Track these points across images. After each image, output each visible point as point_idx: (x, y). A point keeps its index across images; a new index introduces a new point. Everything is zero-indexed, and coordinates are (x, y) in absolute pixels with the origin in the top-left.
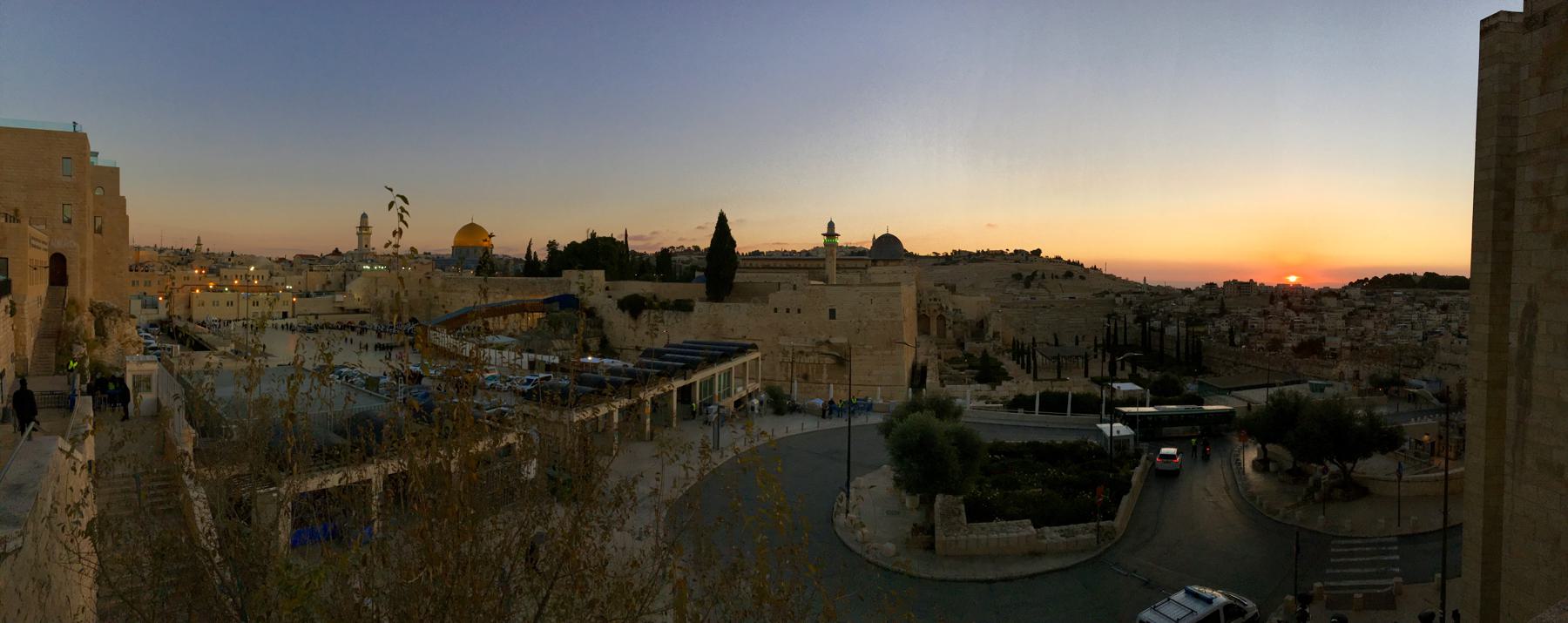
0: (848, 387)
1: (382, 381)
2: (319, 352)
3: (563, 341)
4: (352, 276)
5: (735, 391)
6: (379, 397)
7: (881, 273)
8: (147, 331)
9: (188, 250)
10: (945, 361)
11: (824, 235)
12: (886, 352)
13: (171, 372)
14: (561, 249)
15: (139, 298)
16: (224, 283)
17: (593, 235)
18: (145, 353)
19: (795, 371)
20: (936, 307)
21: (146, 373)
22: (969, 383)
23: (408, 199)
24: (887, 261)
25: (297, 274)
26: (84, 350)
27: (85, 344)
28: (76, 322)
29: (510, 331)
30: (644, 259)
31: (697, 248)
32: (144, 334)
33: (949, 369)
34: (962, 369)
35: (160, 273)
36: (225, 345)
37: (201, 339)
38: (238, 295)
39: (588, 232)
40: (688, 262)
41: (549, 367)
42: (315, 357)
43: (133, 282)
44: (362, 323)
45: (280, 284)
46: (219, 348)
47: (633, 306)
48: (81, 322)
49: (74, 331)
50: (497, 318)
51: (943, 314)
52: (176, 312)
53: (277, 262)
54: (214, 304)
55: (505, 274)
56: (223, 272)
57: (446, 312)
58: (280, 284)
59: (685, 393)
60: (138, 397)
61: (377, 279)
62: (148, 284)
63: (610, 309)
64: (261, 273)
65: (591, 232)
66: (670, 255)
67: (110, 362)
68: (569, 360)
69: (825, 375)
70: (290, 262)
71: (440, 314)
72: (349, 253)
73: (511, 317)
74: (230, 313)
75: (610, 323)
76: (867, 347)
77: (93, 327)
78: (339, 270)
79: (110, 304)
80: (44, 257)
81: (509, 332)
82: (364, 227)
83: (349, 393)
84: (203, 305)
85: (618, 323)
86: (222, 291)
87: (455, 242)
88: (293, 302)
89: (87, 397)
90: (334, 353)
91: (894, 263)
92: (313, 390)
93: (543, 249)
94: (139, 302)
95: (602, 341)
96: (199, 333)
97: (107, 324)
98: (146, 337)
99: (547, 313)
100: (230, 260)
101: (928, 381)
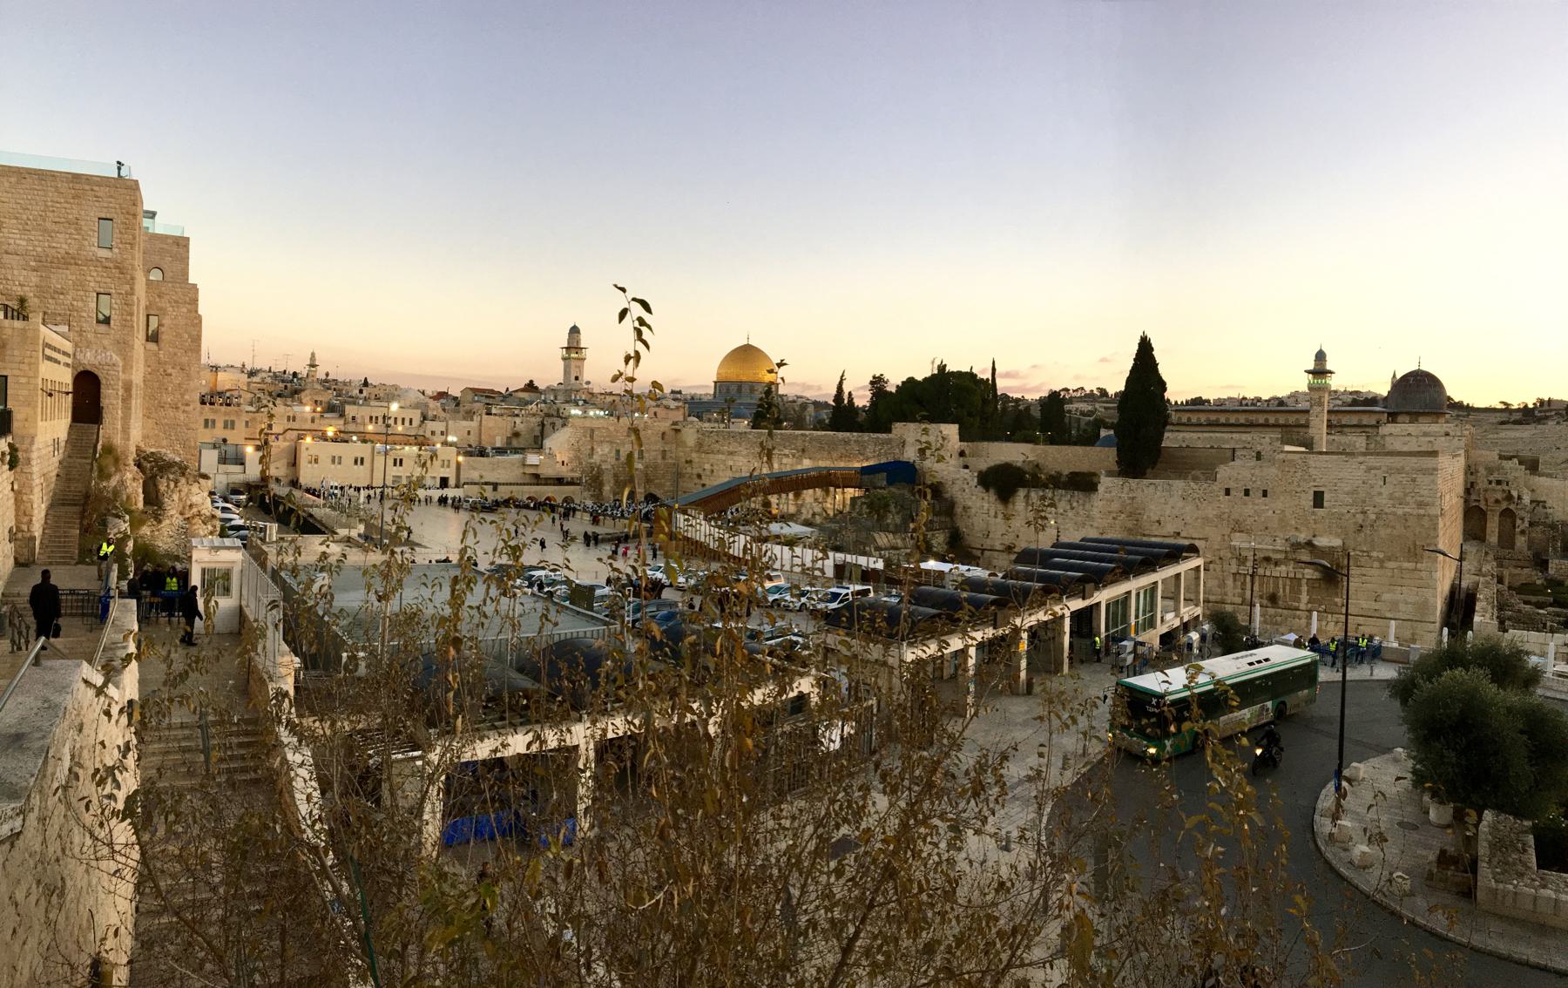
0: (1343, 618)
2: (501, 544)
3: (891, 536)
5: (1162, 618)
7: (1400, 434)
8: (226, 500)
9: (295, 374)
10: (1510, 588)
11: (1308, 372)
12: (1406, 565)
13: (263, 565)
15: (215, 447)
17: (942, 368)
18: (222, 535)
19: (1256, 588)
20: (1499, 496)
22: (1552, 631)
23: (651, 306)
24: (1414, 416)
26: (125, 526)
27: (127, 517)
28: (114, 481)
29: (806, 514)
30: (1021, 407)
31: (1103, 392)
32: (221, 504)
33: (1516, 600)
34: (1540, 605)
35: (250, 408)
37: (311, 516)
38: (373, 448)
40: (1090, 413)
41: (867, 576)
42: (495, 551)
43: (206, 421)
45: (438, 432)
47: (1002, 482)
48: (122, 482)
49: (110, 495)
50: (784, 496)
51: (1512, 507)
54: (333, 462)
55: (799, 424)
57: (704, 485)
59: (1083, 620)
60: (213, 603)
61: (592, 431)
62: (230, 425)
63: (966, 486)
66: (1063, 401)
67: (166, 547)
68: (899, 566)
69: (1304, 597)
71: (694, 490)
73: (808, 495)
75: (966, 508)
76: (1374, 554)
77: (140, 490)
79: (170, 455)
81: (803, 517)
85: (979, 509)
87: (718, 374)
89: (127, 600)
90: (524, 545)
91: (1429, 419)
92: (488, 601)
94: (215, 453)
95: (951, 533)
96: (308, 506)
97: (162, 488)
98: (224, 510)
99: (867, 490)
101: (1477, 619)
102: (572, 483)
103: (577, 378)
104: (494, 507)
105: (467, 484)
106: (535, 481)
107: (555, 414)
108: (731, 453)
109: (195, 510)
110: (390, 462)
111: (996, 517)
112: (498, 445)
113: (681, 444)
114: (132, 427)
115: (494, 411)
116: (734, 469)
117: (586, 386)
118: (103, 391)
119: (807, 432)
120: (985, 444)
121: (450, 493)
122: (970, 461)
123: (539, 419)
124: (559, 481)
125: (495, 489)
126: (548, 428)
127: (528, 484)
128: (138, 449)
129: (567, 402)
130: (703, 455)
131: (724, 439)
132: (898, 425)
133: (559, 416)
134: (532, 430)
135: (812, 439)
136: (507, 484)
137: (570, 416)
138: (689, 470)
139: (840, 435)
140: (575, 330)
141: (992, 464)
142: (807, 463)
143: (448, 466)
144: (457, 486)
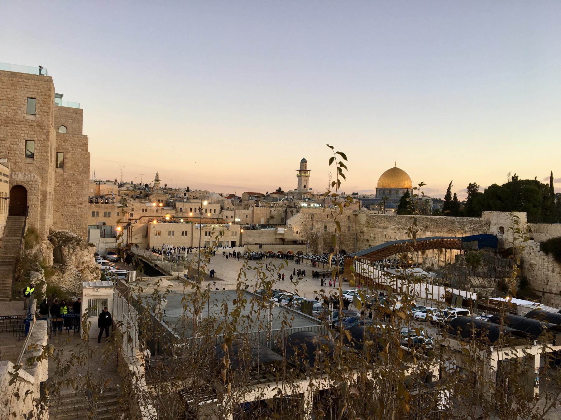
1: (315, 305)
2: (260, 281)
3: (481, 280)
4: (292, 212)
6: (312, 320)
8: (105, 258)
14: (481, 191)
15: (98, 228)
16: (180, 215)
21: (102, 297)
25: (244, 209)
26: (41, 276)
27: (43, 271)
28: (35, 250)
32: (102, 261)
36: (179, 271)
37: (156, 265)
39: (509, 175)
41: (466, 303)
42: (257, 284)
44: (300, 253)
46: (172, 273)
48: (40, 250)
49: (33, 258)
50: (416, 253)
52: (134, 241)
53: (227, 198)
55: (424, 212)
56: (179, 205)
57: (370, 245)
58: (230, 217)
61: (313, 215)
63: (532, 251)
64: (213, 207)
65: (512, 175)
67: (67, 287)
68: (486, 298)
70: (239, 198)
71: (364, 247)
72: (290, 193)
73: (430, 253)
74: (185, 242)
75: (531, 265)
77: (52, 255)
78: (281, 207)
79: (70, 233)
80: (6, 189)
82: (303, 170)
83: (286, 318)
84: (159, 234)
86: (177, 223)
88: (241, 234)
90: (273, 281)
93: (464, 190)
94: (98, 231)
95: (522, 280)
96: (154, 260)
97: (65, 252)
98: (104, 264)
99: (466, 251)
100: (185, 194)
102: (302, 243)
103: (305, 187)
104: (259, 257)
105: (246, 244)
106: (282, 243)
107: (293, 206)
108: (385, 228)
109: (85, 265)
110: (203, 233)
111: (553, 271)
112: (262, 223)
113: (358, 222)
114: (47, 217)
115: (260, 205)
116: (387, 237)
117: (309, 191)
118: (29, 196)
119: (429, 217)
120: (545, 225)
121: (237, 249)
122: (535, 235)
123: (284, 209)
124: (295, 242)
125: (261, 247)
126: (289, 213)
127: (278, 244)
128: (51, 231)
129: (299, 199)
130: (370, 229)
131: (382, 220)
132: (485, 212)
133: (295, 207)
134: (281, 215)
135: (432, 220)
136: (267, 244)
137: (301, 207)
138: (362, 237)
139: (449, 218)
140: (304, 161)
141: (551, 238)
142: (429, 234)
143: (236, 235)
144: (241, 246)
